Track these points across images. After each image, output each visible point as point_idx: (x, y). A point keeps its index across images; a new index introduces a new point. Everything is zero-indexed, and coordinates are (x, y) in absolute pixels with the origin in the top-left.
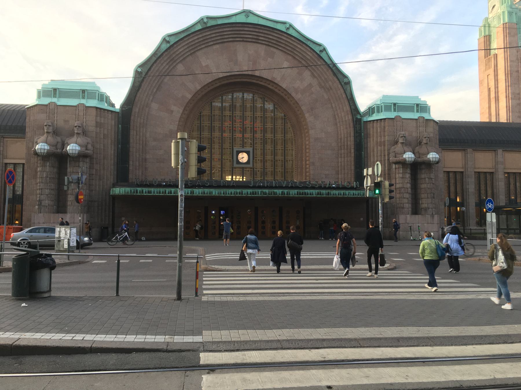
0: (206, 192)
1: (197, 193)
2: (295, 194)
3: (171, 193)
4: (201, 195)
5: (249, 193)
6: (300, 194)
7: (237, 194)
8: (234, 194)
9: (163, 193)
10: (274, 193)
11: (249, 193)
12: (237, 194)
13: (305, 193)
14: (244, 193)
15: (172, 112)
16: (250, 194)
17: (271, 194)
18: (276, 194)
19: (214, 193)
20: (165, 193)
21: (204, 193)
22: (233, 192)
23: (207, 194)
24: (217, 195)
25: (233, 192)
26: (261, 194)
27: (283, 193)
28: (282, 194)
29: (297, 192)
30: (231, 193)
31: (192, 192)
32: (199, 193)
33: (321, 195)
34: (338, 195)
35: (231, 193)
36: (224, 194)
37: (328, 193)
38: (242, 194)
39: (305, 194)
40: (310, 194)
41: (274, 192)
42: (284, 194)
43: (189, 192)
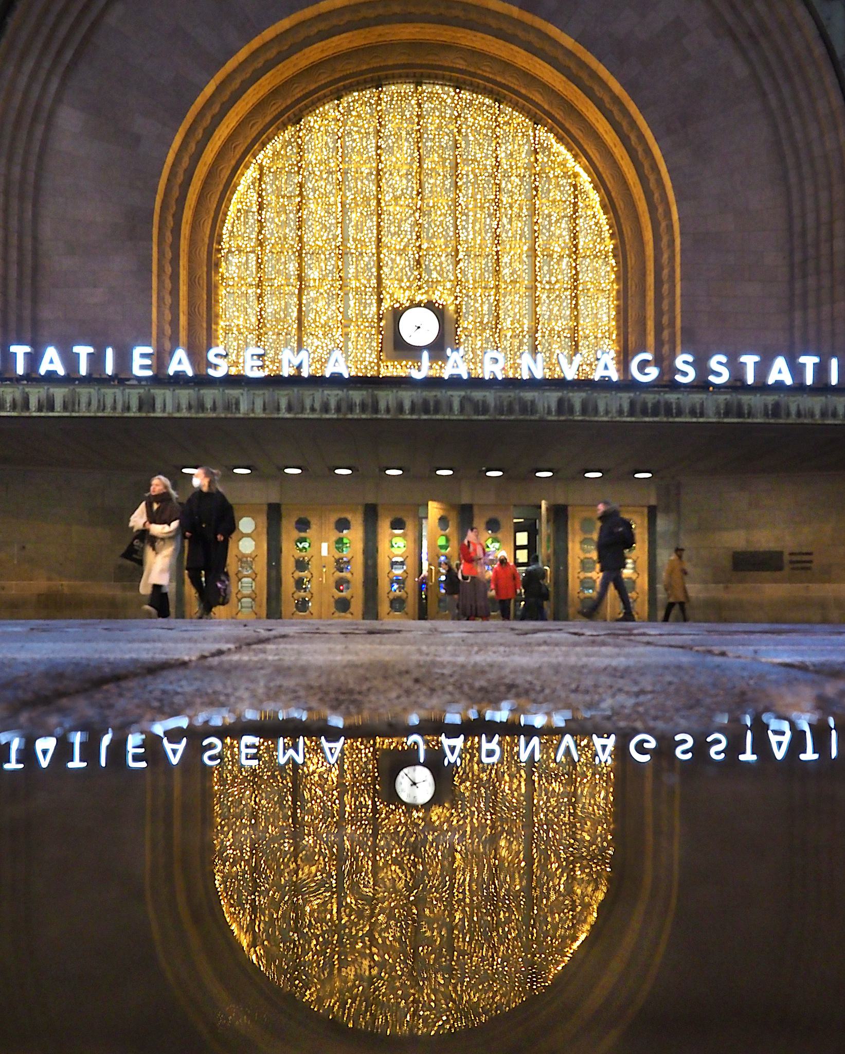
0: (209, 405)
1: (169, 408)
2: (620, 412)
3: (52, 408)
4: (185, 414)
5: (407, 406)
6: (644, 412)
7: (351, 408)
8: (338, 409)
9: (14, 407)
10: (528, 408)
11: (407, 406)
12: (351, 408)
13: (668, 406)
14: (382, 406)
15: (138, 139)
16: (413, 410)
17: (511, 411)
18: (533, 411)
19: (244, 407)
20: (26, 406)
21: (201, 407)
22: (333, 404)
23: (214, 409)
24: (259, 413)
25: (333, 404)
26: (462, 410)
27: (563, 406)
28: (560, 411)
29: (632, 404)
30: (326, 408)
31: (147, 403)
32: (178, 408)
33: (740, 414)
34: (824, 414)
35: (326, 408)
36: (290, 409)
37: (777, 405)
38: (376, 410)
39: (668, 412)
40: (693, 413)
41: (521, 401)
42: (571, 411)
43: (134, 404)
